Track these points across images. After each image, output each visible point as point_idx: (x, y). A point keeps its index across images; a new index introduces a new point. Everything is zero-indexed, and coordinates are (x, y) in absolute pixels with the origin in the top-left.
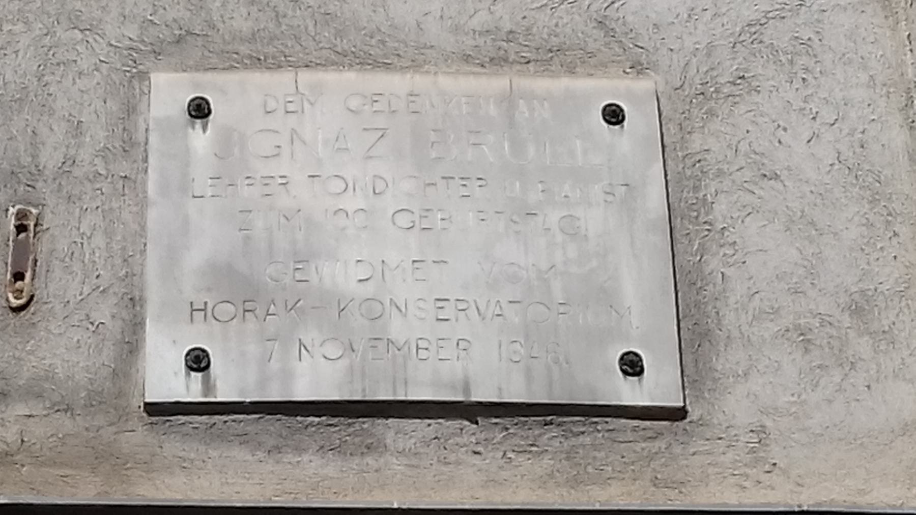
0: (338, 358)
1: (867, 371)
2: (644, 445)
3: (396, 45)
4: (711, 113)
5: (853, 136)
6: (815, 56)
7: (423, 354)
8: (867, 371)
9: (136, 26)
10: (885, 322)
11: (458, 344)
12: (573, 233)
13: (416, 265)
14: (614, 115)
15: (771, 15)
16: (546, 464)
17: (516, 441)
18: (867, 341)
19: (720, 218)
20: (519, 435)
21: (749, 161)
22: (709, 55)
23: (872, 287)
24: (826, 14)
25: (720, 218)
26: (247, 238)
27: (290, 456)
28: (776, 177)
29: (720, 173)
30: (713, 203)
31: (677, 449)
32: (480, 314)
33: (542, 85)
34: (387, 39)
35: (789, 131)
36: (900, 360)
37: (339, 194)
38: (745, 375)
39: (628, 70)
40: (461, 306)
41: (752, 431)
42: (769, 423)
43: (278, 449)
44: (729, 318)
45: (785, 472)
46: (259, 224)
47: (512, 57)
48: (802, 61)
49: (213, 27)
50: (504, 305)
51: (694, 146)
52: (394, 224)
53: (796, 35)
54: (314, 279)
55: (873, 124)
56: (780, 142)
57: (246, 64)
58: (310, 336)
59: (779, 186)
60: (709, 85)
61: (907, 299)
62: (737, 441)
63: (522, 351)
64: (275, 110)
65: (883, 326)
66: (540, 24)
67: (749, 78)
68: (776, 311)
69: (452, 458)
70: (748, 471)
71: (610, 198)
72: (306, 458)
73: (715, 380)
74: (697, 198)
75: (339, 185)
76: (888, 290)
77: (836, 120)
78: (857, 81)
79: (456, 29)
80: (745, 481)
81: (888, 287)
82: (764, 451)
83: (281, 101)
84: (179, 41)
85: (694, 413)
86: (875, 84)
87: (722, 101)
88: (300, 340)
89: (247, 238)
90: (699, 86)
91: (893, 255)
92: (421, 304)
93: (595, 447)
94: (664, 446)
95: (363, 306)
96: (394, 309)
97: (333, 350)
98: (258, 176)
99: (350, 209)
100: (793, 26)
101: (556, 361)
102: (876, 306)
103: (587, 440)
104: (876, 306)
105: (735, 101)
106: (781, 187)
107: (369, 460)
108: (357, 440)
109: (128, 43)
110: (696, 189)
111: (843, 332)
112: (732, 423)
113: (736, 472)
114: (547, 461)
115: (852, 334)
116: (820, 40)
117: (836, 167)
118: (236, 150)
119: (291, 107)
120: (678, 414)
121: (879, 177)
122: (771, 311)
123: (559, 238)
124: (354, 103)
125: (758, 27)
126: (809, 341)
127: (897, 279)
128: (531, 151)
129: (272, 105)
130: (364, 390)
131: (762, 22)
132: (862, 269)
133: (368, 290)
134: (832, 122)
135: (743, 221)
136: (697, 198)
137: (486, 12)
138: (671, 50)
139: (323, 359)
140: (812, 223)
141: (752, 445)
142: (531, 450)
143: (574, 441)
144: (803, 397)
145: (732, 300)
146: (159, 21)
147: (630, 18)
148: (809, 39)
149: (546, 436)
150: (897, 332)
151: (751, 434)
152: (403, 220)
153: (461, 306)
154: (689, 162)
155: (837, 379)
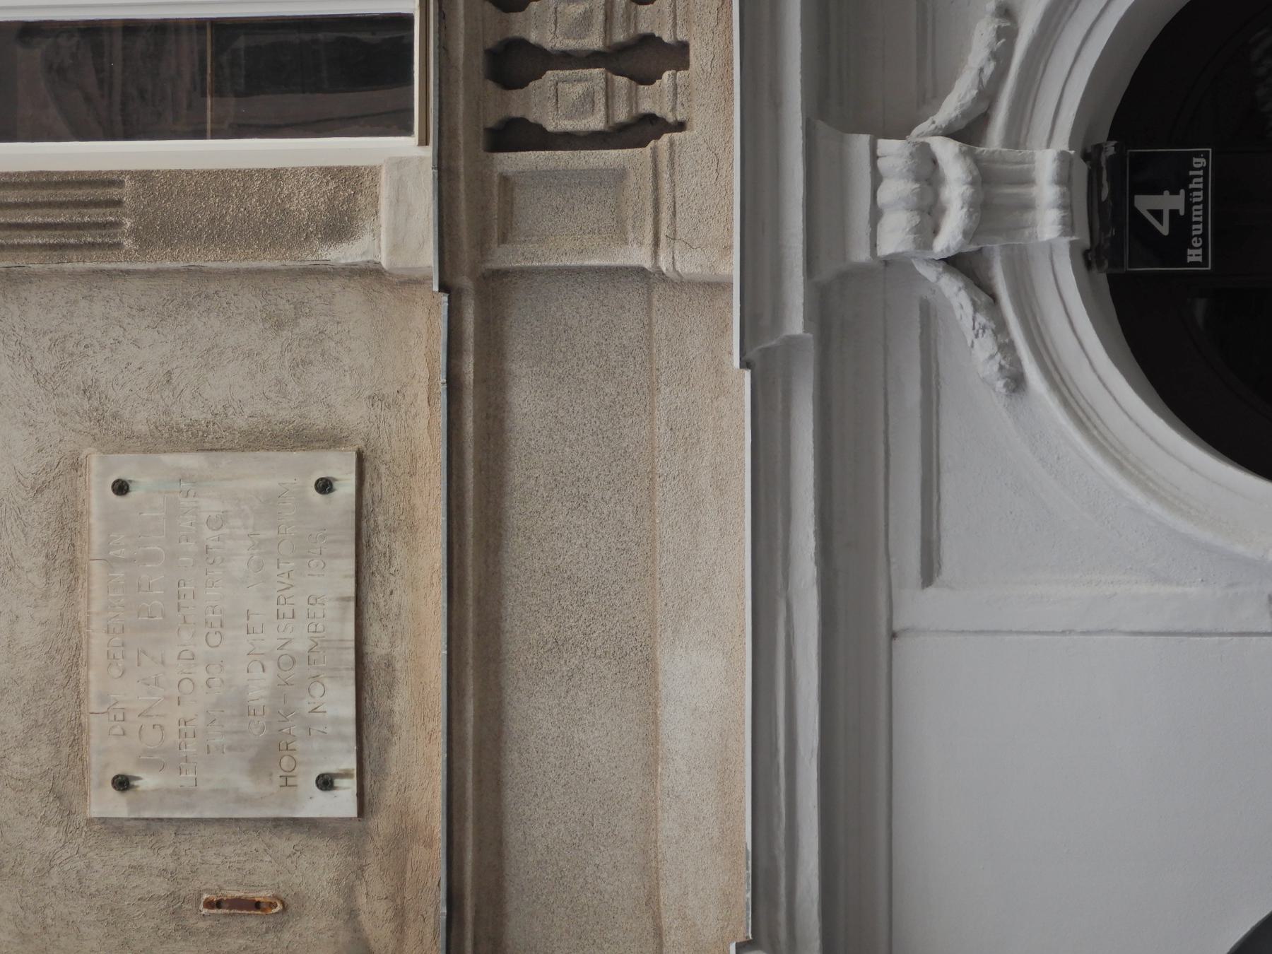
0: (323, 685)
1: (326, 322)
2: (384, 479)
3: (60, 640)
4: (115, 416)
5: (134, 316)
6: (65, 337)
7: (320, 628)
8: (326, 322)
9: (47, 829)
10: (287, 307)
11: (312, 604)
12: (220, 521)
13: (251, 631)
14: (121, 488)
15: (29, 366)
16: (398, 546)
17: (382, 567)
18: (302, 320)
19: (204, 415)
20: (377, 564)
21: (156, 391)
22: (65, 415)
23: (259, 313)
24: (28, 326)
25: (204, 415)
26: (230, 748)
27: (395, 719)
28: (169, 373)
29: (166, 412)
30: (191, 419)
31: (387, 457)
32: (289, 588)
33: (97, 538)
34: (56, 647)
35: (130, 361)
36: (317, 299)
37: (193, 684)
38: (329, 407)
39: (79, 473)
40: (282, 601)
41: (373, 405)
42: (367, 393)
43: (391, 728)
44: (283, 415)
45: (404, 386)
46: (218, 740)
47: (68, 556)
48: (70, 345)
49: (46, 773)
50: (280, 572)
51: (143, 430)
52: (217, 646)
53: (46, 349)
54: (262, 702)
55: (124, 300)
56: (140, 368)
57: (79, 749)
58: (306, 706)
59: (177, 372)
60: (91, 416)
61: (269, 290)
62: (380, 416)
63: (316, 561)
64: (122, 729)
65: (290, 309)
66: (39, 535)
67: (84, 386)
68: (279, 382)
69: (395, 610)
70: (403, 410)
71: (191, 493)
72: (396, 709)
73: (334, 428)
74: (187, 431)
75: (187, 686)
76: (261, 302)
77: (120, 326)
78: (87, 308)
79: (46, 596)
80: (411, 412)
81: (259, 302)
82: (388, 398)
83: (115, 723)
84: (59, 798)
85: (361, 444)
86: (90, 296)
87: (105, 407)
88: (309, 712)
89: (230, 748)
90: (92, 423)
91: (233, 296)
92: (281, 629)
93: (386, 512)
94: (384, 466)
95: (284, 668)
96: (286, 647)
97: (318, 690)
98: (179, 741)
99: (205, 676)
100: (39, 351)
101: (323, 537)
102: (274, 312)
103: (380, 518)
104: (274, 312)
105: (104, 397)
106: (179, 370)
107: (398, 666)
108: (382, 675)
109: (61, 835)
110: (179, 431)
111: (295, 337)
112: (366, 418)
113: (404, 419)
114: (396, 546)
115: (297, 330)
116: (51, 332)
117: (160, 330)
118: (156, 757)
119: (120, 717)
120: (361, 458)
121: (168, 300)
122: (279, 386)
123: (225, 531)
124: (115, 672)
125: (40, 377)
126: (302, 361)
127: (253, 296)
128: (153, 548)
129: (118, 730)
130: (347, 669)
131: (36, 373)
132: (245, 319)
133: (270, 665)
134: (122, 329)
135: (206, 400)
136: (187, 431)
137: (30, 575)
138: (61, 441)
139: (324, 697)
140: (208, 350)
141: (383, 406)
142: (389, 556)
143: (381, 527)
144: (346, 368)
145: (270, 412)
146: (42, 812)
147: (33, 469)
148: (50, 340)
149: (378, 545)
150: (295, 300)
151: (375, 406)
152: (214, 639)
153: (282, 601)
154: (158, 434)
155: (333, 344)
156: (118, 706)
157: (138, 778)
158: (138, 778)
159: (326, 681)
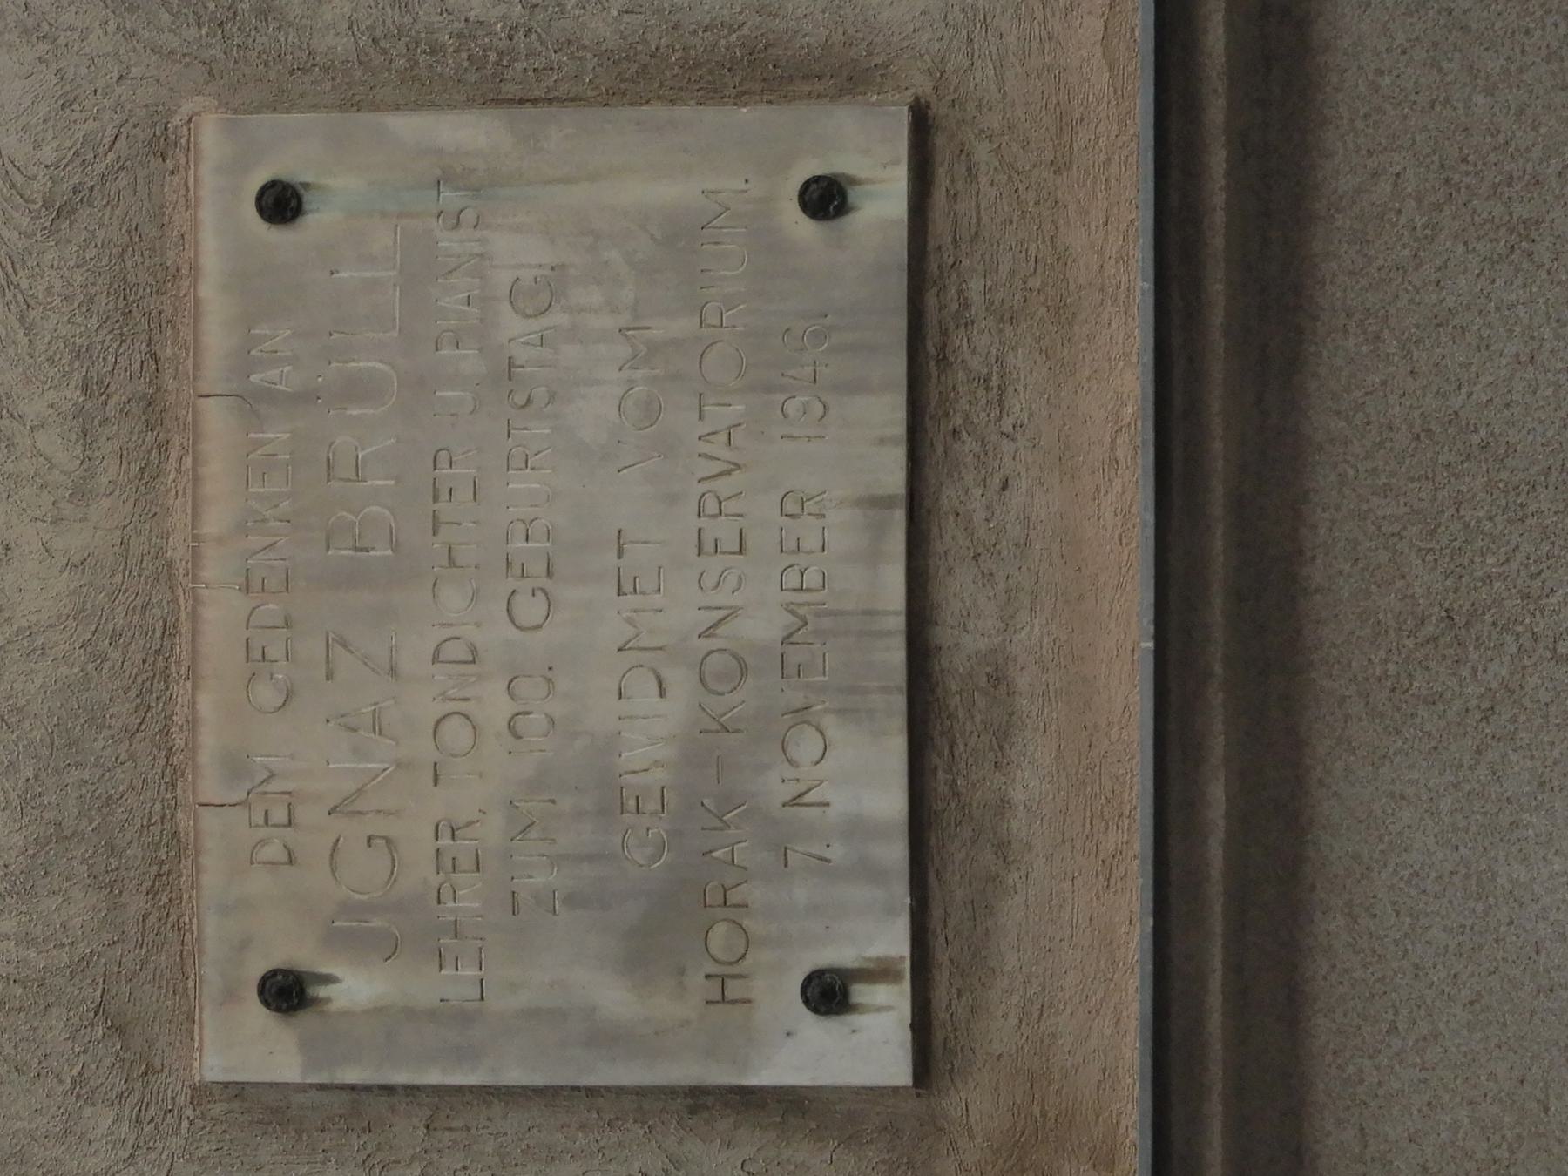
7: (812, 578)
13: (627, 587)
26: (572, 900)
27: (1015, 824)
32: (728, 473)
33: (217, 338)
37: (474, 728)
39: (170, 164)
40: (711, 506)
43: (1002, 848)
52: (539, 627)
54: (659, 776)
58: (775, 787)
71: (469, 216)
72: (1018, 795)
79: (81, 493)
83: (263, 832)
89: (572, 900)
92: (709, 581)
97: (806, 746)
98: (435, 880)
108: (981, 702)
118: (376, 923)
119: (279, 815)
123: (558, 318)
124: (267, 695)
129: (273, 851)
133: (680, 679)
152: (531, 610)
153: (711, 506)
156: (274, 786)
157: (328, 979)
158: (328, 979)
159: (830, 723)
